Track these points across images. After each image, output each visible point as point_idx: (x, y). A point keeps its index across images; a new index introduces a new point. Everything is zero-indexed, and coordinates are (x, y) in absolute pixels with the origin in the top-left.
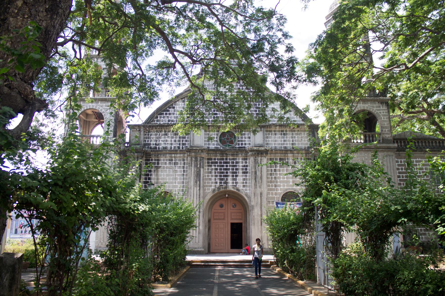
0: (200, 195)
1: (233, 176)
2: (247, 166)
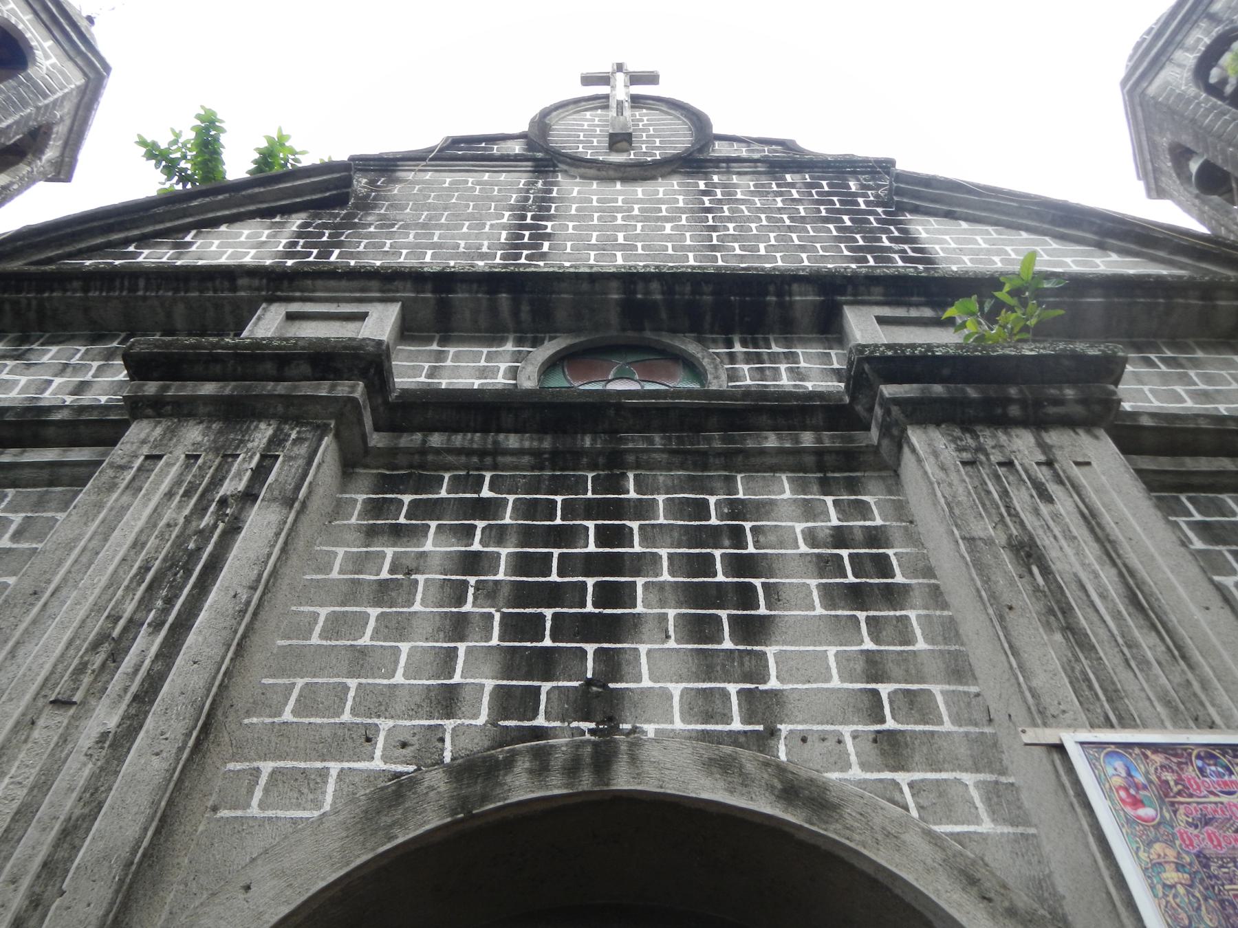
0: (71, 833)
1: (700, 629)
2: (875, 537)
